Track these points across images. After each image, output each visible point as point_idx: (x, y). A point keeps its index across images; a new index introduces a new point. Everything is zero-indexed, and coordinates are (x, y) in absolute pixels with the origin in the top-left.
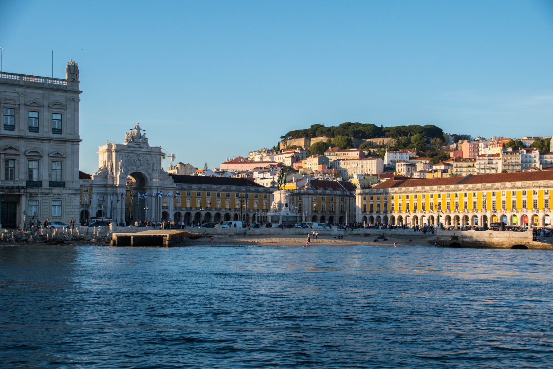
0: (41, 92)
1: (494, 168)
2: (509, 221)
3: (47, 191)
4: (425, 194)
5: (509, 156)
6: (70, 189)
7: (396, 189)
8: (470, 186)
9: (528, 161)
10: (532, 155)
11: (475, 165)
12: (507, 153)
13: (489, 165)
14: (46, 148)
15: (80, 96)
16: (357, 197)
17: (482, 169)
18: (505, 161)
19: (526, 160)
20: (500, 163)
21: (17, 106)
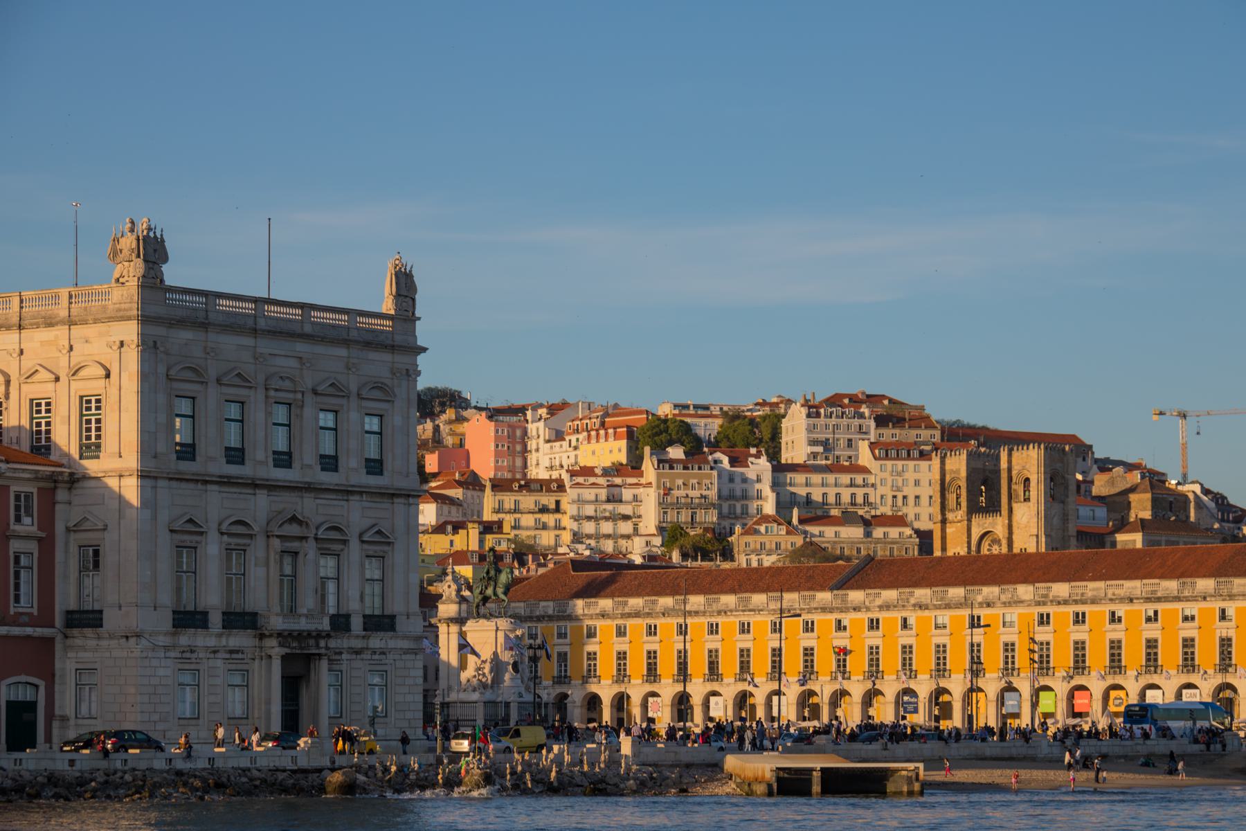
0: (342, 352)
1: (626, 518)
2: (1097, 706)
3: (358, 644)
4: (720, 620)
5: (679, 476)
6: (405, 637)
7: (605, 603)
8: (890, 595)
9: (738, 493)
10: (751, 473)
11: (564, 506)
12: (671, 464)
13: (609, 507)
14: (356, 515)
15: (421, 359)
16: (443, 628)
17: (589, 518)
18: (668, 491)
19: (732, 491)
20: (650, 498)
21: (299, 396)
